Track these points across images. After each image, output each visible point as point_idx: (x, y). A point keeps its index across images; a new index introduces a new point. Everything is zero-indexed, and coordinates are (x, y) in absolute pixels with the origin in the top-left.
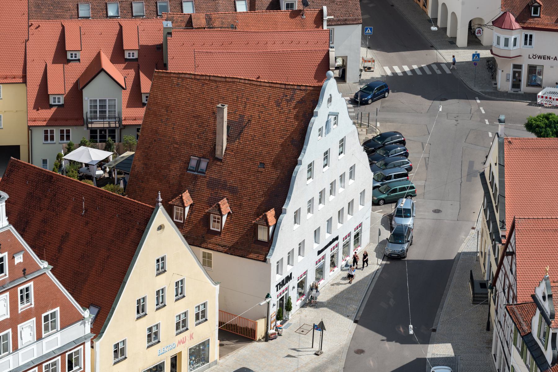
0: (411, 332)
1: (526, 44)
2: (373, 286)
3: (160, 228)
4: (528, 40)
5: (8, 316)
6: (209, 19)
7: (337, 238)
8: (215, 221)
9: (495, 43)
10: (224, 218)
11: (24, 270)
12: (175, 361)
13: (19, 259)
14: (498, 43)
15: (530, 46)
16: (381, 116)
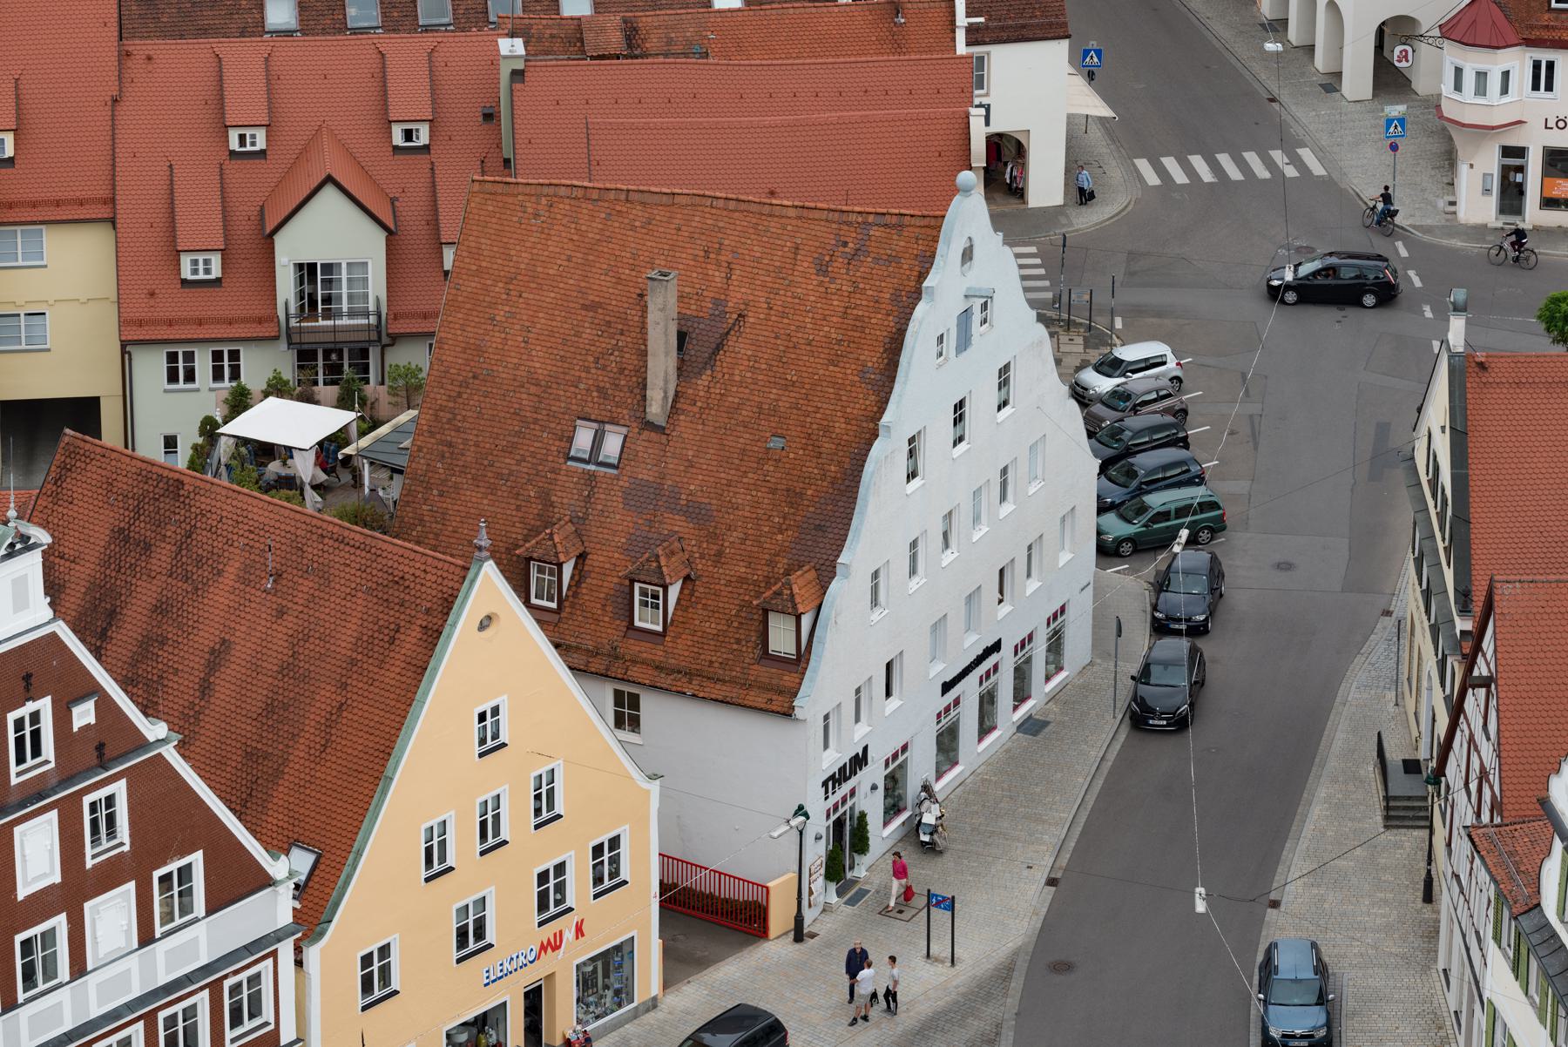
0: (1201, 907)
1: (1536, 87)
2: (1100, 783)
3: (486, 623)
4: (1543, 78)
5: (57, 878)
6: (631, 33)
7: (996, 647)
8: (645, 604)
9: (1447, 88)
10: (674, 592)
11: (100, 747)
12: (534, 1000)
13: (84, 715)
14: (1458, 87)
15: (1549, 94)
16: (1127, 296)
